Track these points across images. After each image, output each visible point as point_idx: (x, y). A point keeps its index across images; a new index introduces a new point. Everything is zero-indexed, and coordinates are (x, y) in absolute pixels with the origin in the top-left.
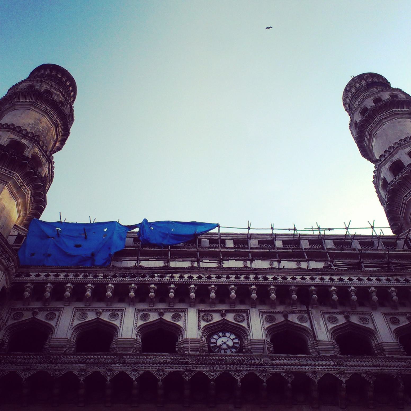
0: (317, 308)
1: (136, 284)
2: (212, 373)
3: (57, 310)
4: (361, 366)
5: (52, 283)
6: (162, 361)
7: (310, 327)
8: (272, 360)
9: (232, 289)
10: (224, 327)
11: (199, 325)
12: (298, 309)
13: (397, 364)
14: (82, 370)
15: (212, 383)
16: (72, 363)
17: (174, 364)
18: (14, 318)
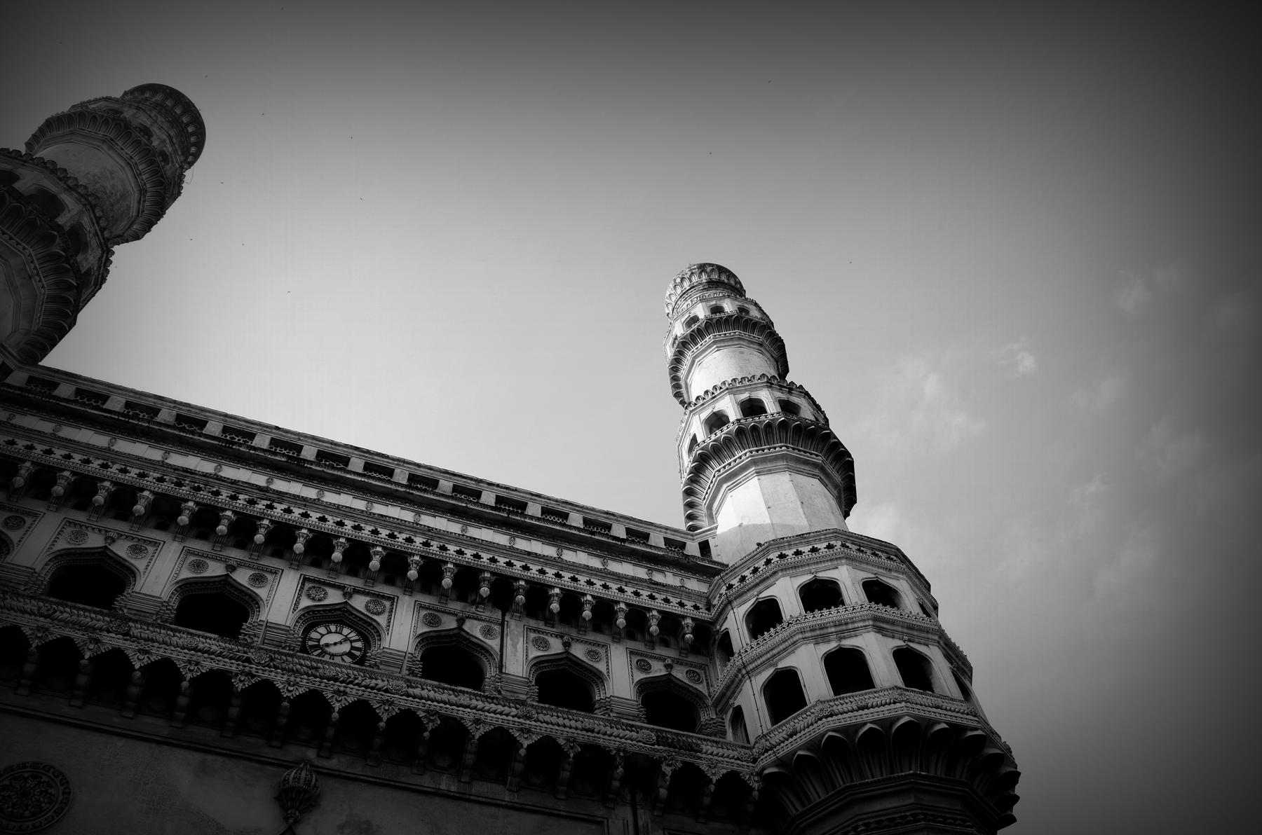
0: (520, 619)
1: (197, 503)
2: (290, 686)
3: (29, 514)
4: (561, 725)
6: (201, 646)
7: (497, 649)
9: (376, 553)
10: (341, 616)
12: (487, 614)
13: (622, 733)
14: (39, 629)
15: (286, 704)
16: (24, 612)
17: (224, 657)
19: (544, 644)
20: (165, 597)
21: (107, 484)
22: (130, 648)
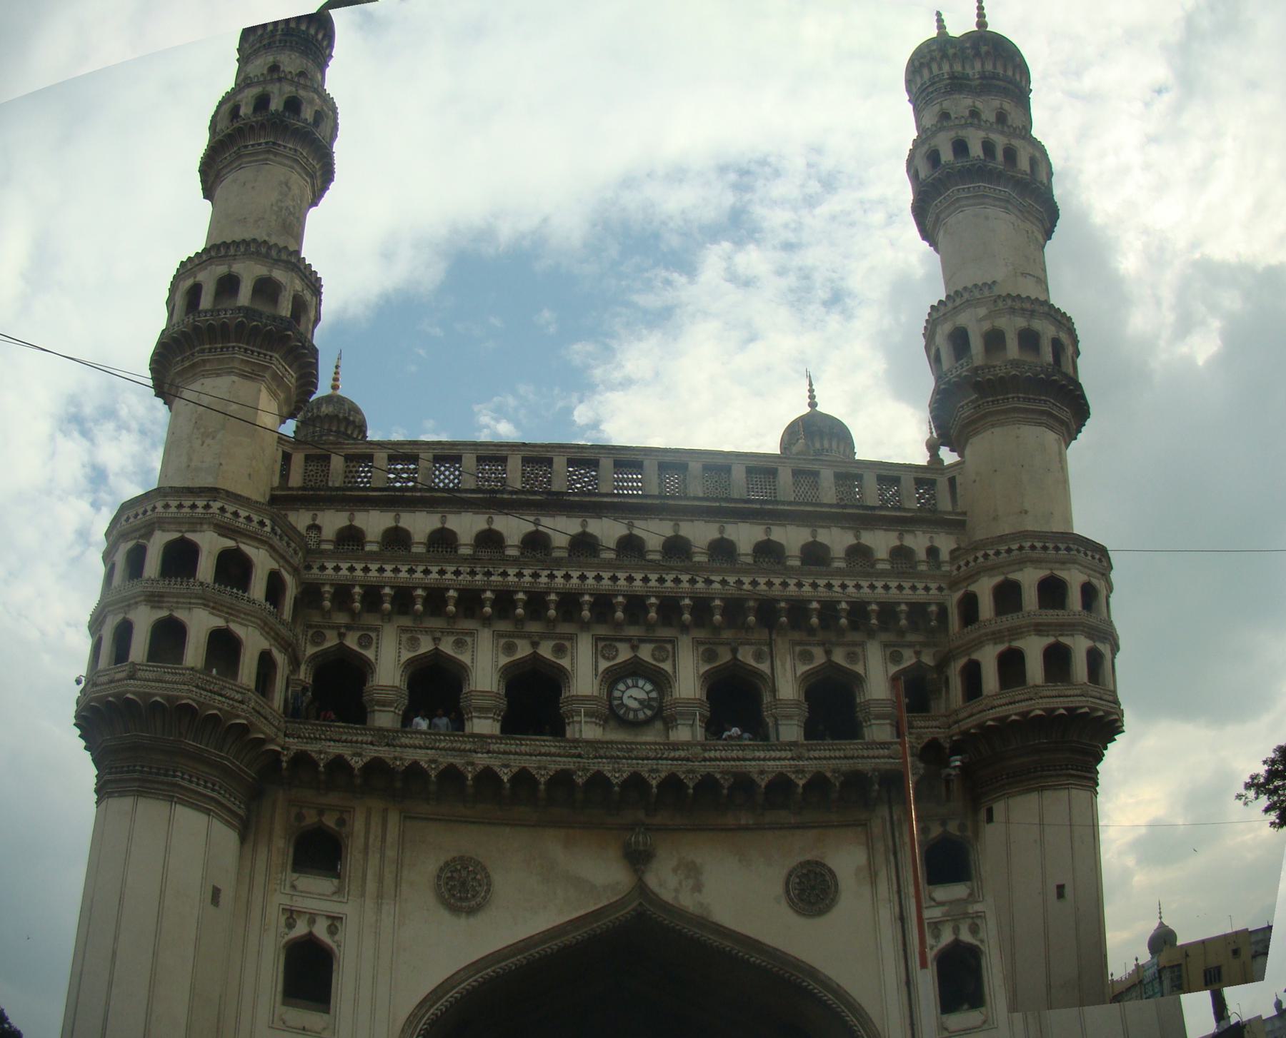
5: (361, 586)
7: (768, 671)
8: (705, 750)
9: (652, 605)
10: (635, 670)
11: (596, 669)
13: (876, 752)
15: (616, 788)
18: (315, 643)
19: (806, 657)
20: (495, 690)
21: (419, 592)
22: (495, 763)
